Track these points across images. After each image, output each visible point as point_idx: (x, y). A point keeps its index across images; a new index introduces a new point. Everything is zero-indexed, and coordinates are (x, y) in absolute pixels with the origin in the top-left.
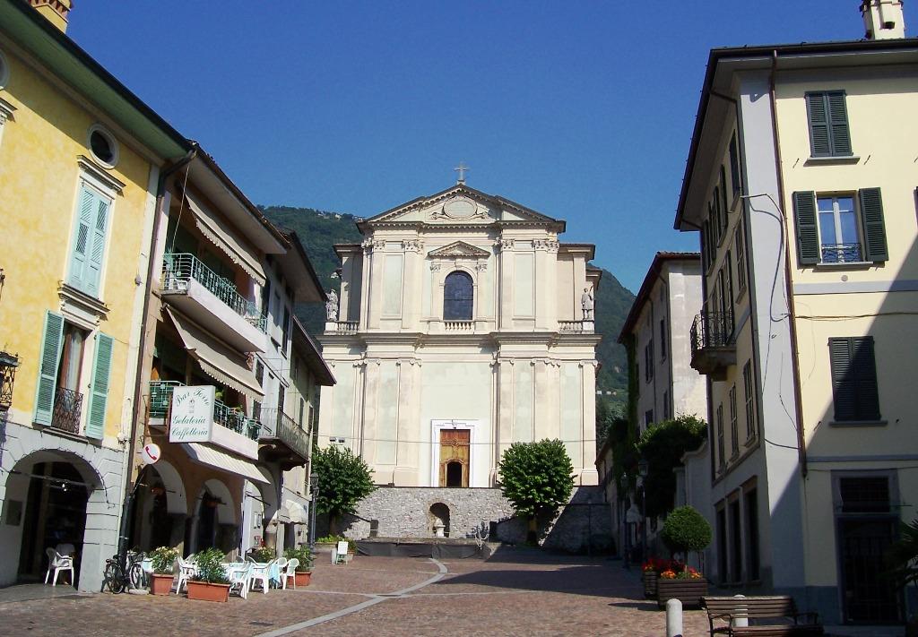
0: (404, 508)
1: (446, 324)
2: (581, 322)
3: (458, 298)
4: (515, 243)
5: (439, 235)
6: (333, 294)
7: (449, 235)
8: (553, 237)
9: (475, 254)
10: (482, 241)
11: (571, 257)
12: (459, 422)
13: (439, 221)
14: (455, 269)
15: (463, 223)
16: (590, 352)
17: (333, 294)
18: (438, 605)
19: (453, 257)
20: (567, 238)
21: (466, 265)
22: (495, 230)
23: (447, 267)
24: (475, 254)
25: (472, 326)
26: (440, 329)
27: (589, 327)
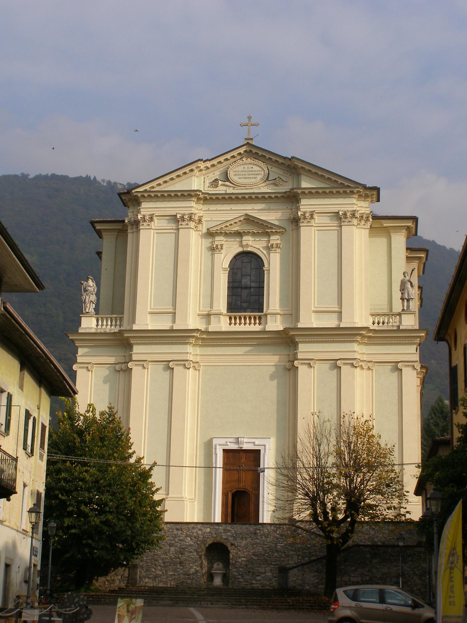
0: (172, 549)
1: (230, 318)
2: (400, 314)
3: (246, 288)
4: (315, 216)
5: (219, 207)
6: (91, 283)
7: (234, 207)
8: (363, 206)
9: (264, 229)
10: (273, 216)
11: (387, 233)
12: (245, 440)
13: (221, 189)
14: (240, 250)
15: (256, 191)
16: (410, 352)
17: (91, 283)
18: (189, 561)
19: (239, 234)
20: (381, 209)
21: (255, 244)
22: (292, 198)
23: (231, 249)
24: (264, 229)
25: (263, 321)
26: (223, 324)
27: (410, 321)
